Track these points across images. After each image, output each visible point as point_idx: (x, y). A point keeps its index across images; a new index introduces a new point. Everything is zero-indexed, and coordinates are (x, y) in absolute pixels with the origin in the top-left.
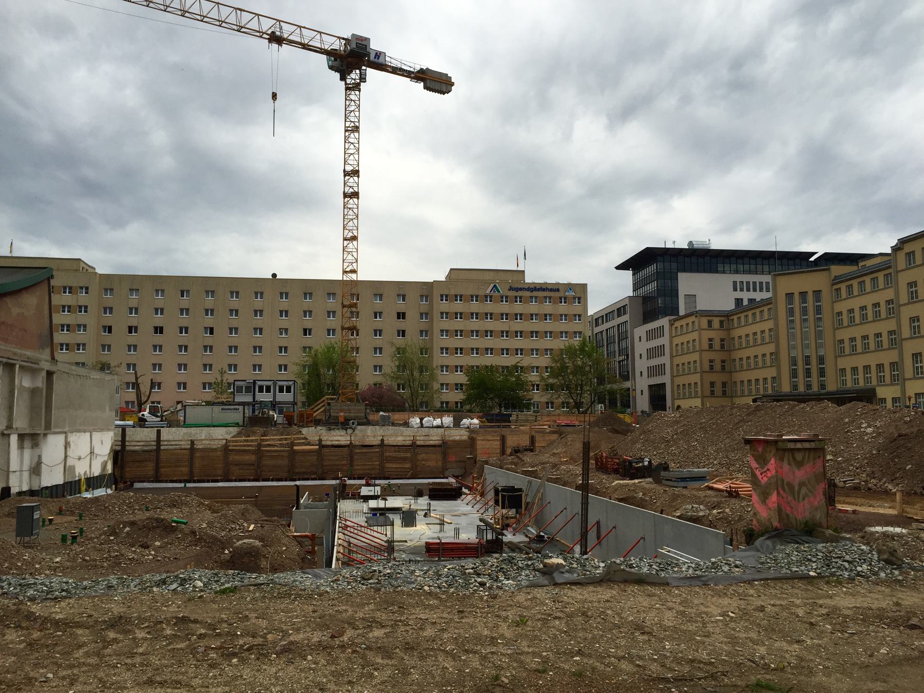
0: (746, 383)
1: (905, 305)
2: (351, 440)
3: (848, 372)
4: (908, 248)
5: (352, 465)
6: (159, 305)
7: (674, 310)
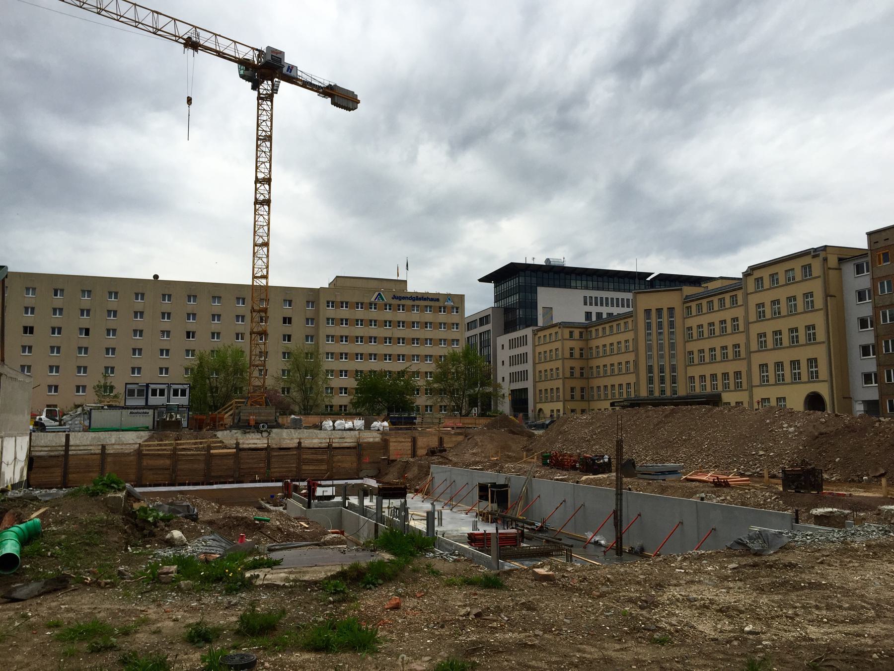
0: (602, 388)
1: (753, 323)
2: (268, 443)
3: (697, 380)
4: (757, 274)
5: (269, 467)
6: (216, 311)
7: (534, 322)
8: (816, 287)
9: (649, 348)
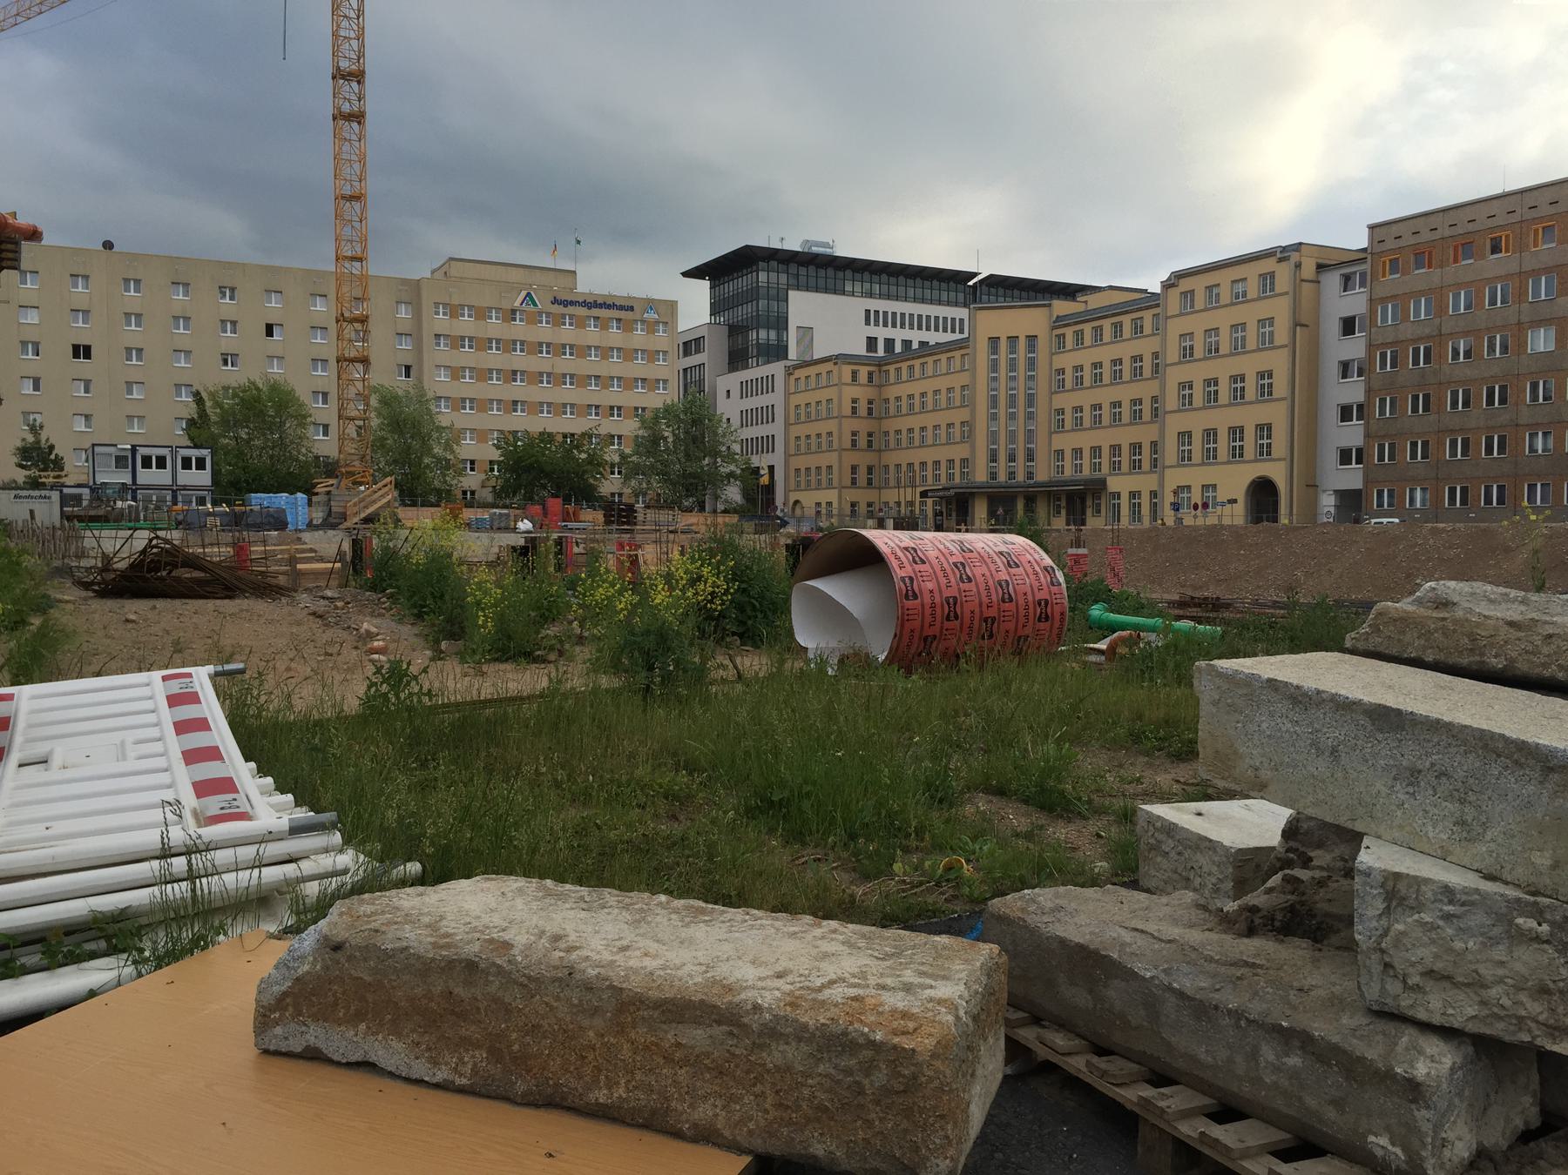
3: (1068, 454)
4: (1185, 285)
7: (779, 352)
8: (1280, 309)
9: (994, 402)
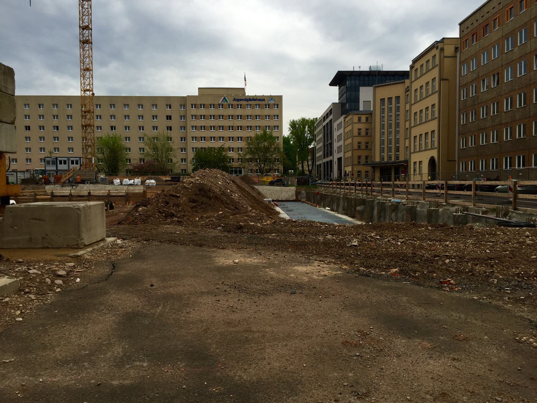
9: (382, 127)
